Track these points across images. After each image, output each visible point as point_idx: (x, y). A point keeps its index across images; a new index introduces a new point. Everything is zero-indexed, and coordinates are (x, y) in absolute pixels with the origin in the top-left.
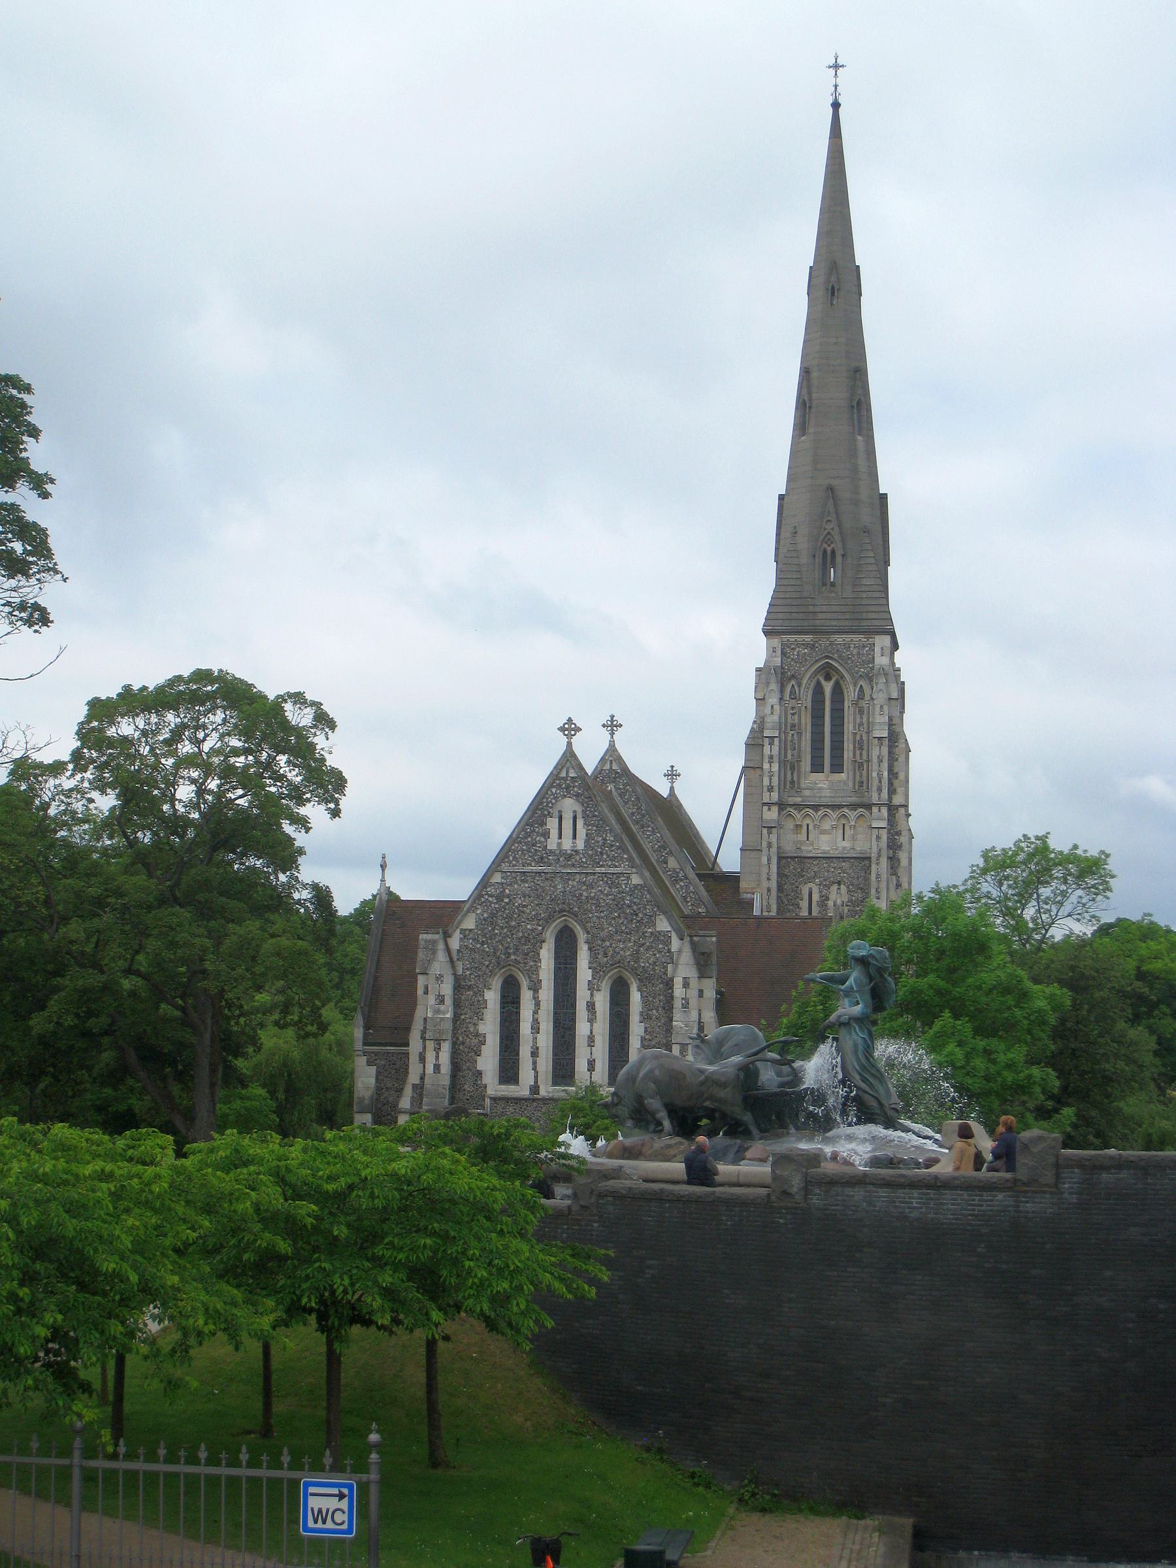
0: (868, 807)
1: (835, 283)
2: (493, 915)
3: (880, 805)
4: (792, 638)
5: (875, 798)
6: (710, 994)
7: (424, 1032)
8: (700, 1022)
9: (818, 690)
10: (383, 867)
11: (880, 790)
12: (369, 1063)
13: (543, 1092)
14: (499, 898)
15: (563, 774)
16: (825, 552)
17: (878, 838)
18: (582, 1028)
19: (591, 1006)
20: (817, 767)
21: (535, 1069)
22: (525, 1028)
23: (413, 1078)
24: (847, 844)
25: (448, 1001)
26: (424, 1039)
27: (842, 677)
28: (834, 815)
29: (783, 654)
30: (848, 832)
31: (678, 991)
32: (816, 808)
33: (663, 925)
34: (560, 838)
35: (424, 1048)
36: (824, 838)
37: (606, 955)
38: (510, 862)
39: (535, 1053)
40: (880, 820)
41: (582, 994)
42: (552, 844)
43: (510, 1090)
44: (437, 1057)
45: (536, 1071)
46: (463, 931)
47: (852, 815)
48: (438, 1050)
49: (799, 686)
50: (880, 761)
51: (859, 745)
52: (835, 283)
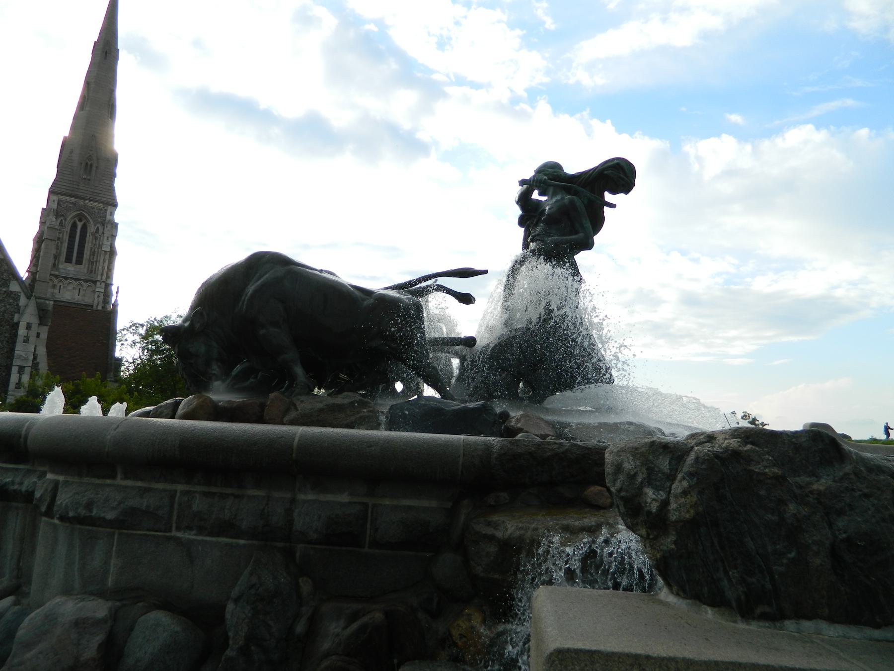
0: (95, 282)
1: (106, 51)
3: (101, 282)
4: (64, 198)
5: (99, 278)
6: (44, 336)
8: (34, 354)
9: (74, 226)
11: (102, 275)
16: (87, 164)
17: (99, 296)
20: (68, 260)
24: (80, 297)
27: (88, 221)
28: (75, 283)
29: (58, 204)
30: (82, 292)
31: (22, 331)
32: (66, 278)
36: (68, 293)
47: (85, 285)
49: (65, 220)
50: (104, 261)
51: (93, 253)
52: (106, 51)
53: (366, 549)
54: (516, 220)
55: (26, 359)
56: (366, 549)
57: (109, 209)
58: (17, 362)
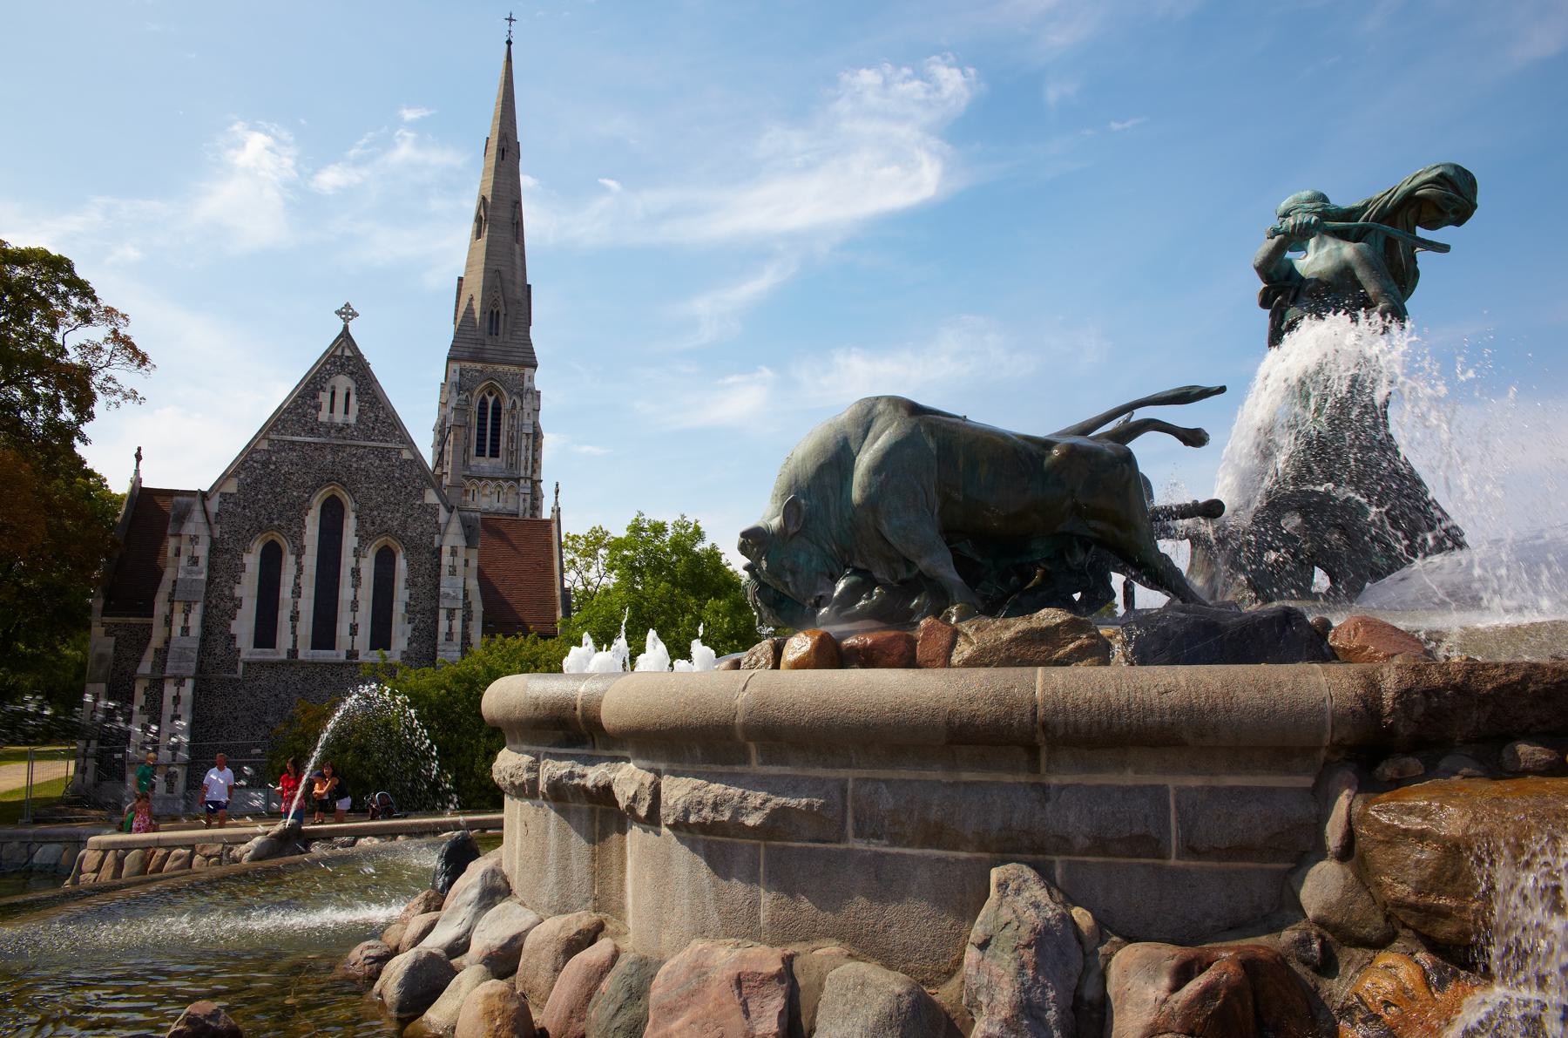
0: (518, 480)
2: (257, 481)
4: (468, 365)
5: (522, 473)
6: (474, 563)
7: (172, 594)
9: (484, 403)
10: (138, 457)
12: (107, 634)
13: (301, 656)
14: (265, 464)
15: (339, 353)
18: (346, 593)
19: (356, 572)
20: (480, 452)
21: (294, 633)
22: (286, 592)
23: (156, 641)
24: (501, 505)
25: (203, 563)
26: (171, 601)
28: (493, 484)
31: (446, 559)
33: (431, 497)
34: (332, 411)
35: (172, 611)
36: (485, 500)
37: (373, 523)
38: (278, 432)
39: (295, 617)
40: (525, 487)
41: (347, 561)
42: (324, 416)
43: (267, 655)
44: (186, 620)
45: (296, 633)
46: (222, 495)
47: (506, 485)
48: (187, 613)
51: (511, 439)
53: (1173, 862)
54: (1256, 299)
55: (455, 598)
56: (1173, 862)
57: (527, 371)
58: (445, 603)
